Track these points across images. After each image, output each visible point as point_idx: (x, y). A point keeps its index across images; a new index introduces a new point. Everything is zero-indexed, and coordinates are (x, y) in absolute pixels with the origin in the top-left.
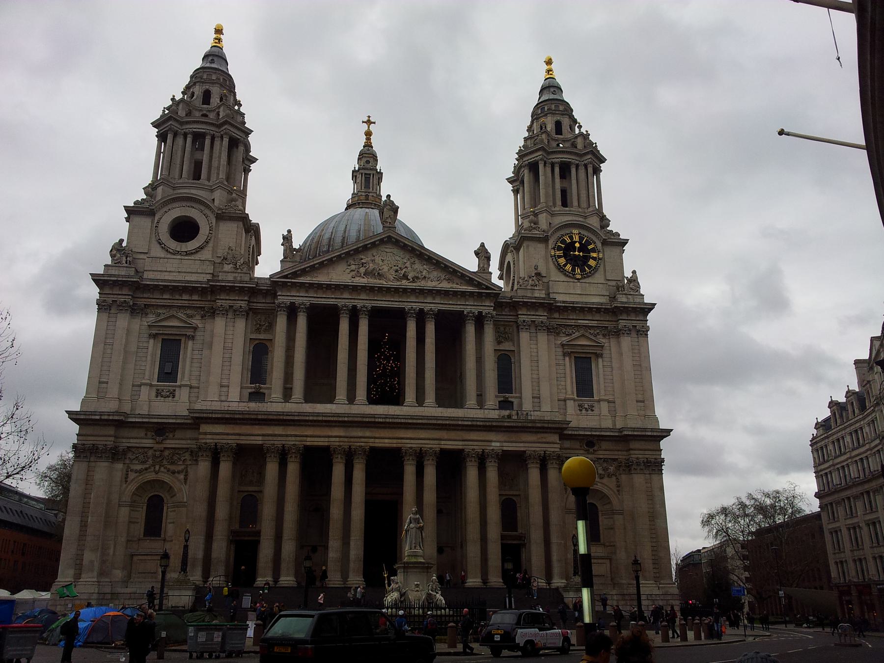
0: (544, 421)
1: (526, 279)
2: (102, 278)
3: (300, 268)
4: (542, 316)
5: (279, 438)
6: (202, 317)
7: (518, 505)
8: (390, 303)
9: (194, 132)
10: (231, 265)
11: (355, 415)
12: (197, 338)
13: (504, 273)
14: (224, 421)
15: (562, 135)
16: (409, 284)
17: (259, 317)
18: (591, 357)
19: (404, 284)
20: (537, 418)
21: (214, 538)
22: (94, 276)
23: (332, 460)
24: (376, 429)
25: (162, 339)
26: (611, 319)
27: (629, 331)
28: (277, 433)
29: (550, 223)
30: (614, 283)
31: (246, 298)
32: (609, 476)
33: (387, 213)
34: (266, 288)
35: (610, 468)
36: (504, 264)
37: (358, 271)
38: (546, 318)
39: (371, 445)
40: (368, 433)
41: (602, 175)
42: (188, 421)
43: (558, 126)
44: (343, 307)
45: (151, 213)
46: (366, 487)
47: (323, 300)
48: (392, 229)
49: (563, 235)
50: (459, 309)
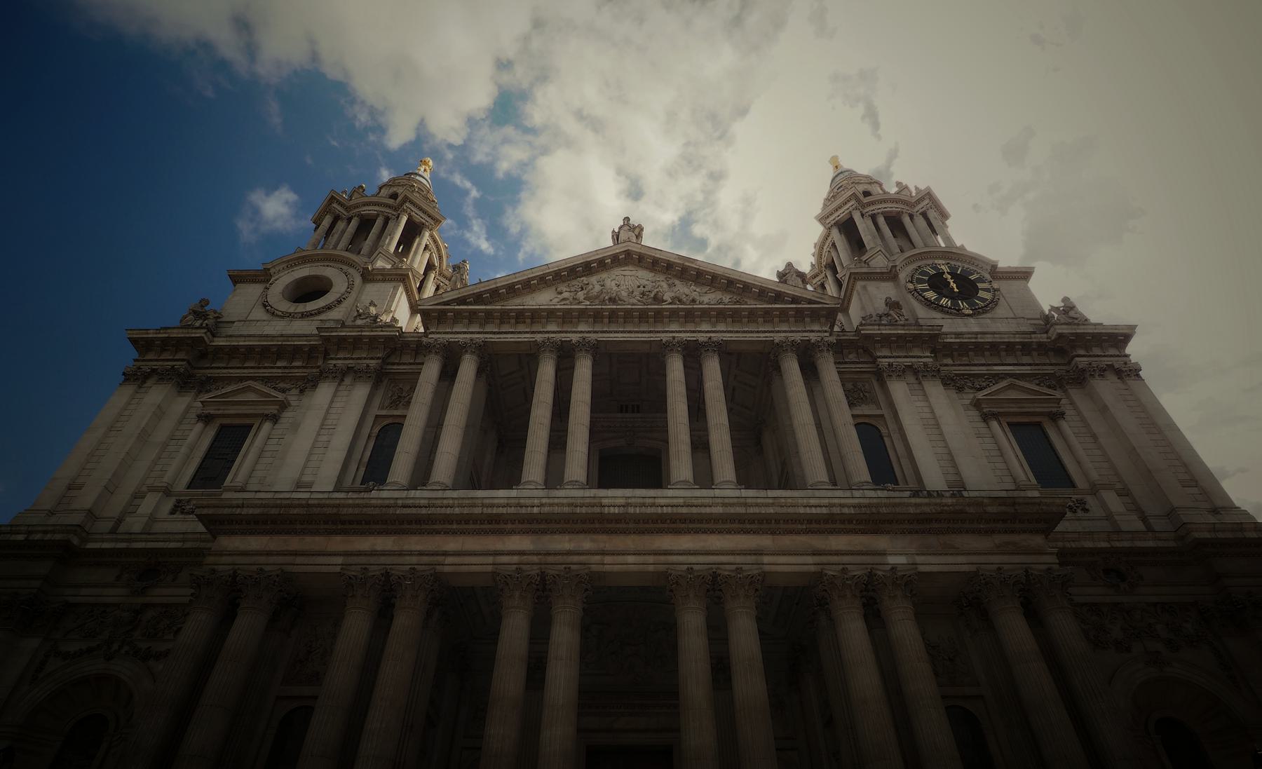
3: (472, 292)
4: (923, 357)
5: (383, 560)
8: (633, 335)
9: (362, 215)
10: (367, 320)
18: (1039, 424)
22: (133, 334)
24: (604, 537)
25: (222, 427)
28: (379, 548)
37: (573, 298)
38: (931, 360)
39: (595, 568)
40: (586, 543)
50: (764, 339)
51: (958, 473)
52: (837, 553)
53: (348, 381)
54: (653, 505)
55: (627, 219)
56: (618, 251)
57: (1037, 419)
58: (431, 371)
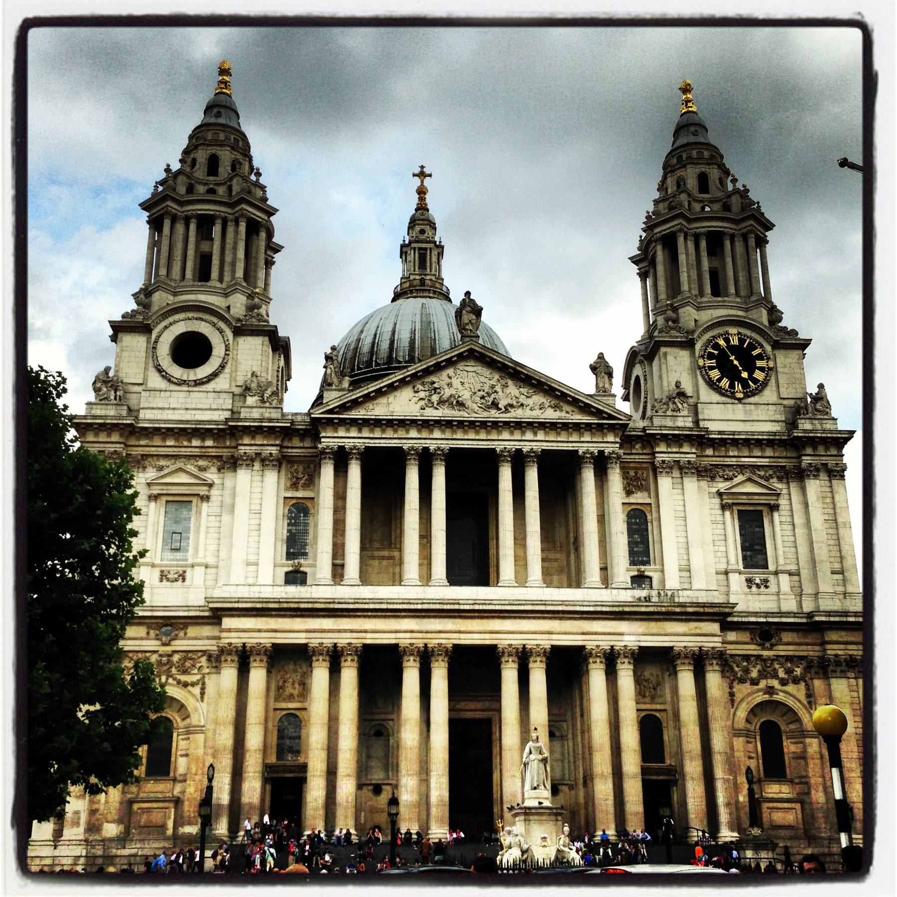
0: (698, 605)
1: (664, 401)
2: (84, 421)
3: (350, 399)
4: (688, 454)
6: (219, 470)
7: (664, 724)
8: (475, 442)
9: (199, 215)
10: (256, 398)
11: (432, 601)
12: (213, 498)
13: (631, 391)
14: (254, 613)
15: (708, 193)
16: (502, 415)
17: (296, 467)
18: (761, 511)
19: (494, 416)
20: (688, 600)
21: (245, 775)
23: (401, 664)
25: (167, 502)
26: (789, 455)
27: (815, 471)
28: (325, 627)
29: (696, 320)
30: (792, 402)
31: (278, 442)
32: (796, 681)
33: (467, 317)
34: (304, 427)
35: (795, 669)
36: (630, 379)
38: (695, 456)
41: (769, 248)
42: (206, 614)
43: (703, 182)
44: (410, 450)
45: (145, 329)
46: (449, 700)
47: (382, 441)
48: (474, 339)
49: (714, 337)
51: (689, 560)
52: (596, 634)
53: (257, 466)
54: (489, 604)
55: (468, 294)
56: (462, 350)
57: (760, 508)
58: (327, 472)
